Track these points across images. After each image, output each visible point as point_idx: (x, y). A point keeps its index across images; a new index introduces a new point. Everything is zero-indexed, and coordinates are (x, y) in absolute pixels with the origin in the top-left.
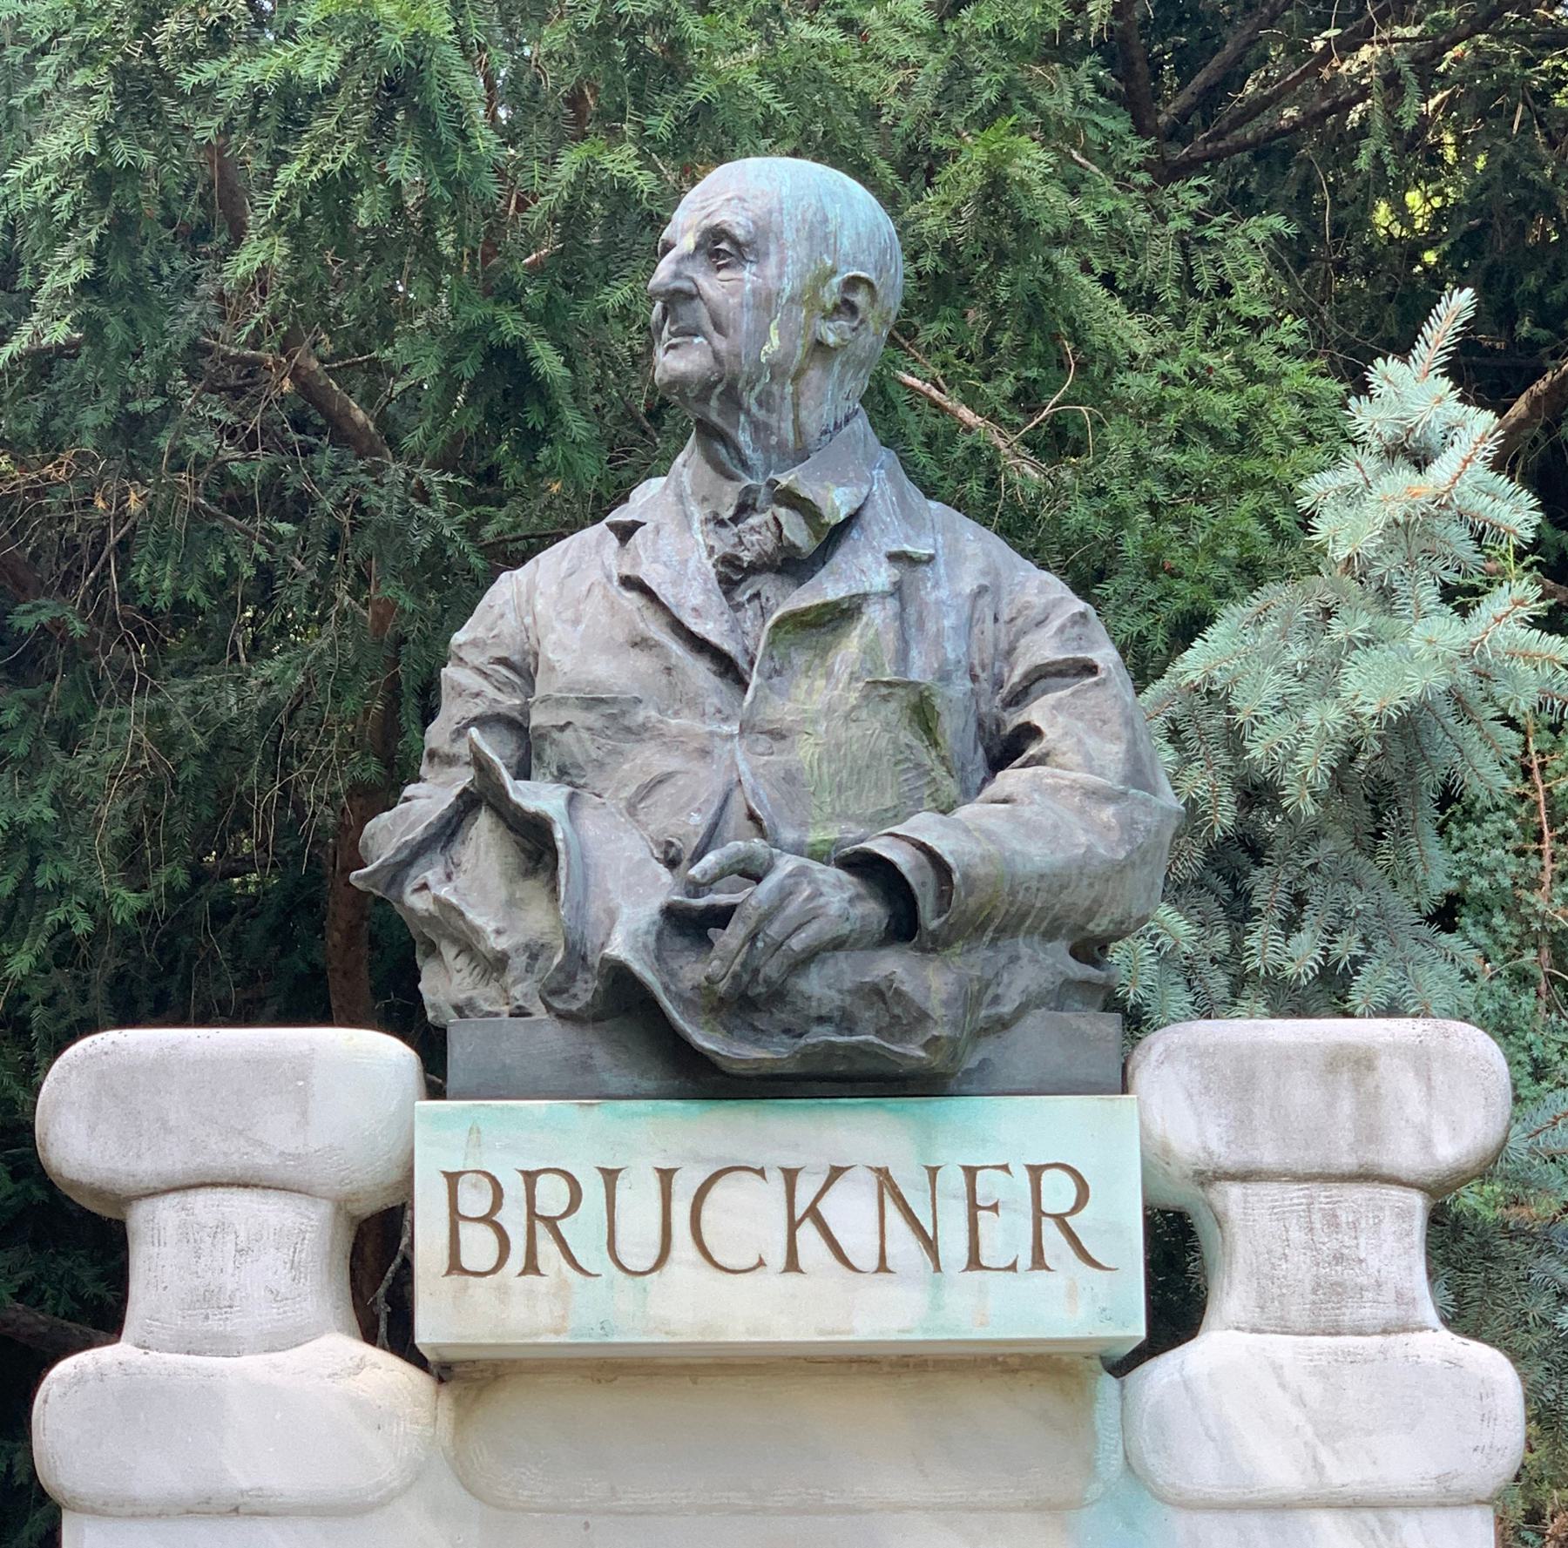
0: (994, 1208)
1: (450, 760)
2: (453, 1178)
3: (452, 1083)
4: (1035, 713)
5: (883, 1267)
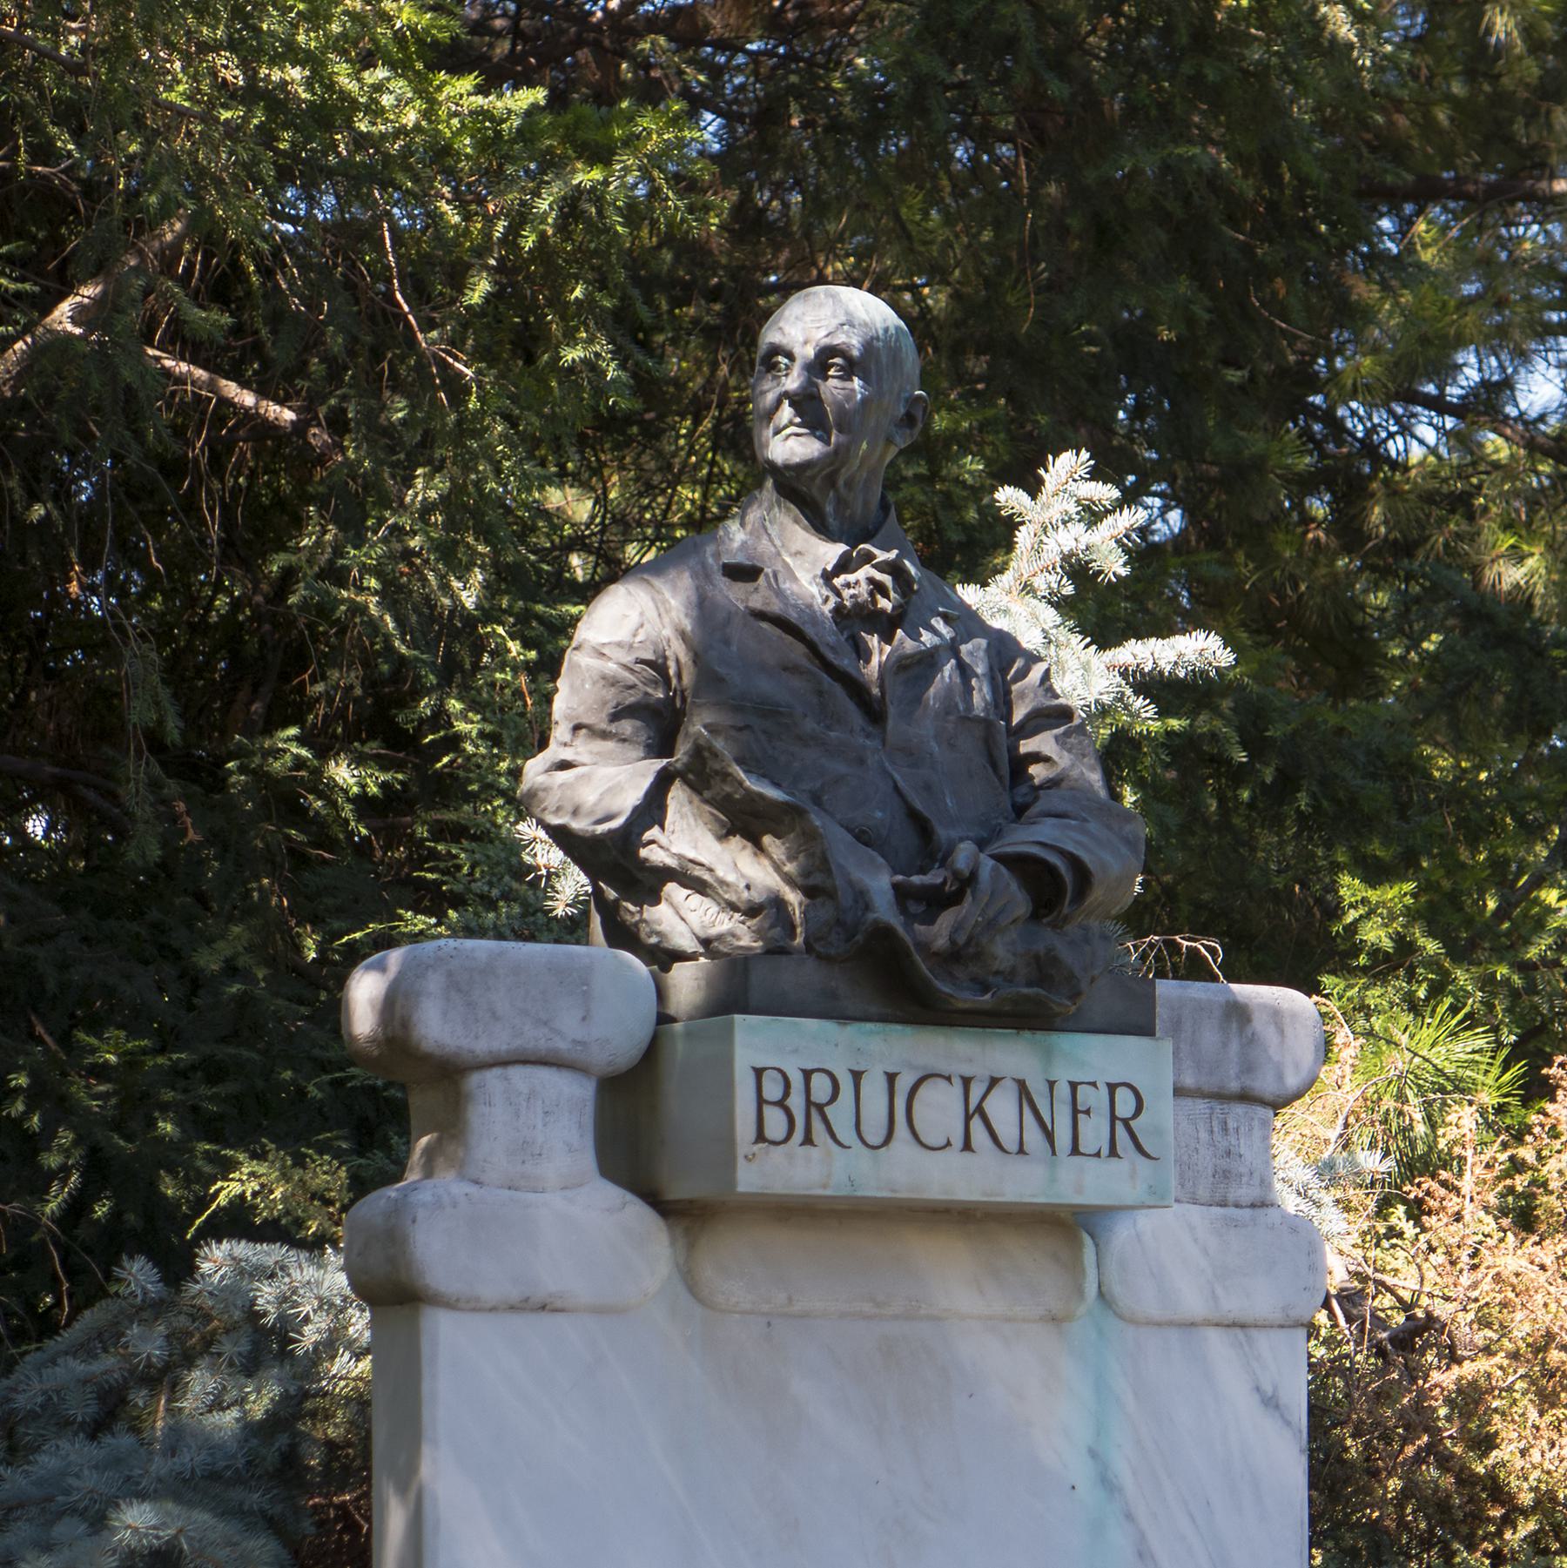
0: (1087, 1112)
2: (759, 1073)
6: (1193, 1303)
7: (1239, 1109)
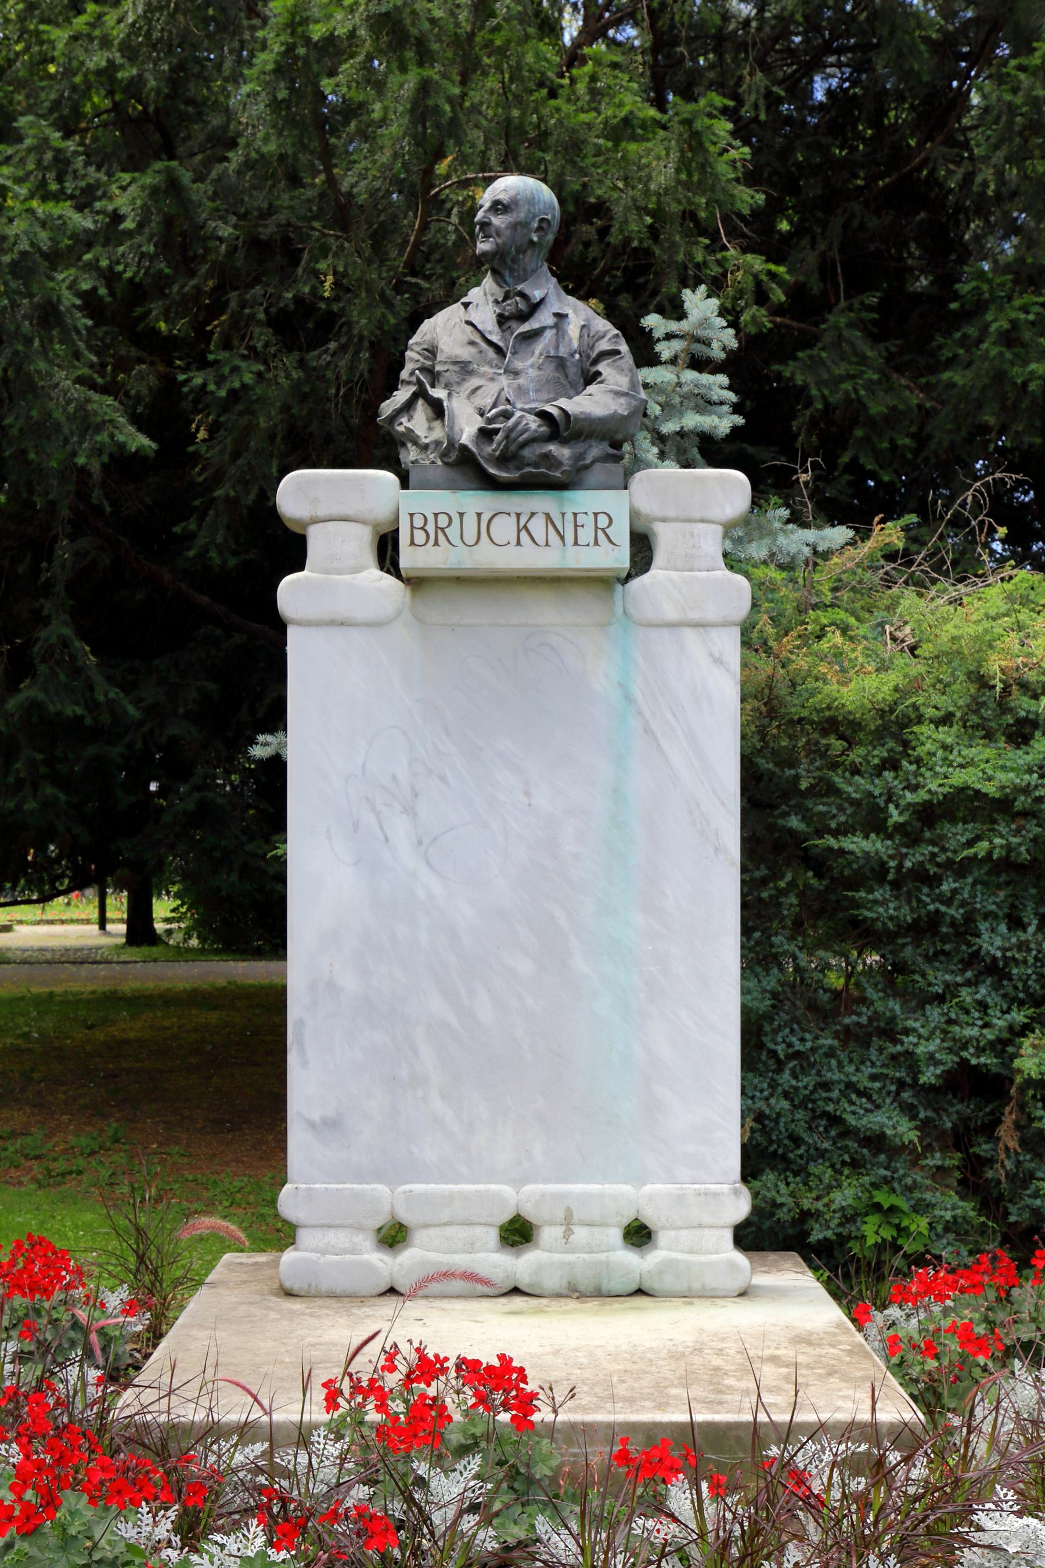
1: (409, 383)
2: (412, 515)
3: (411, 484)
4: (602, 367)
5: (547, 545)
6: (671, 613)
7: (701, 526)
